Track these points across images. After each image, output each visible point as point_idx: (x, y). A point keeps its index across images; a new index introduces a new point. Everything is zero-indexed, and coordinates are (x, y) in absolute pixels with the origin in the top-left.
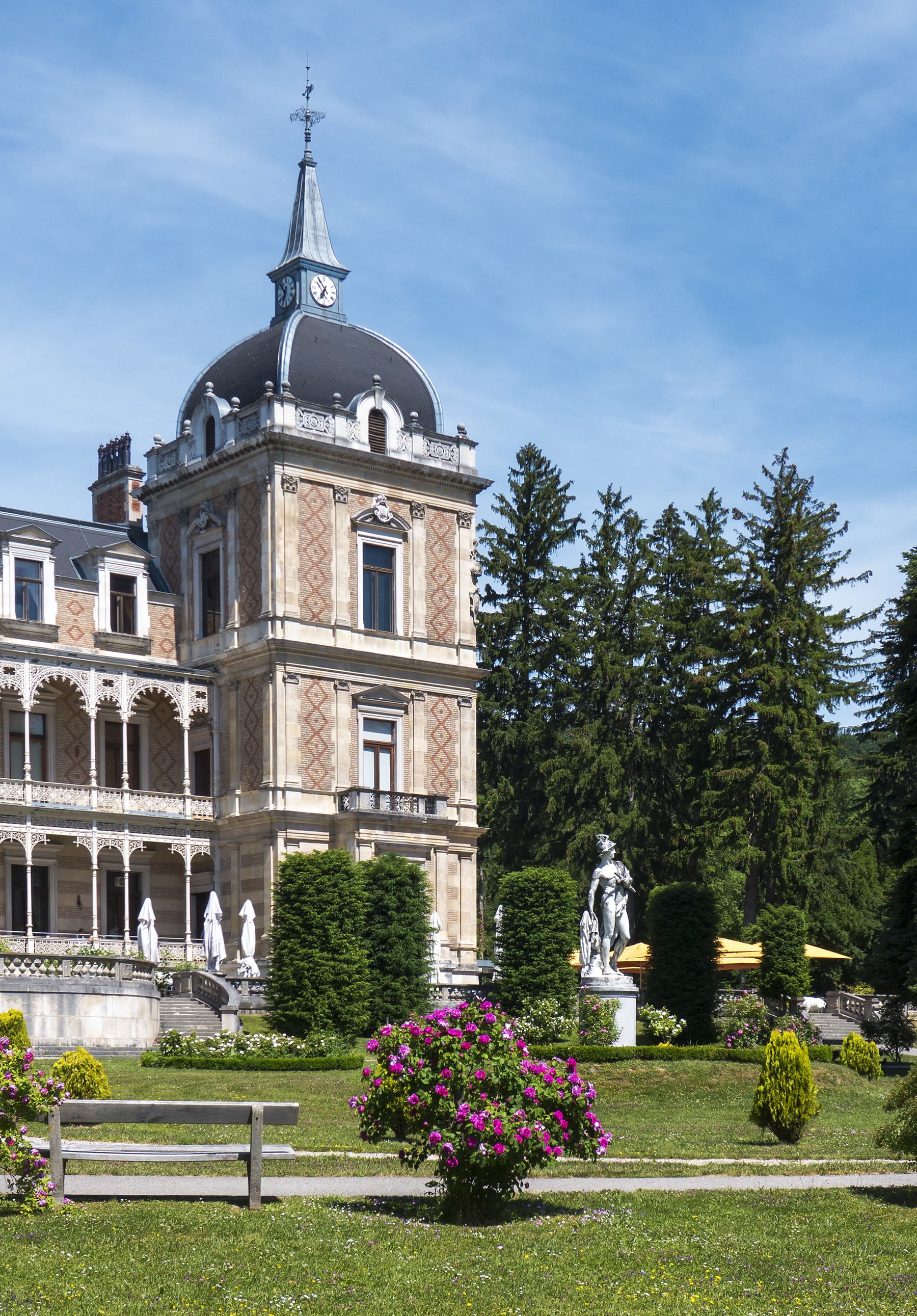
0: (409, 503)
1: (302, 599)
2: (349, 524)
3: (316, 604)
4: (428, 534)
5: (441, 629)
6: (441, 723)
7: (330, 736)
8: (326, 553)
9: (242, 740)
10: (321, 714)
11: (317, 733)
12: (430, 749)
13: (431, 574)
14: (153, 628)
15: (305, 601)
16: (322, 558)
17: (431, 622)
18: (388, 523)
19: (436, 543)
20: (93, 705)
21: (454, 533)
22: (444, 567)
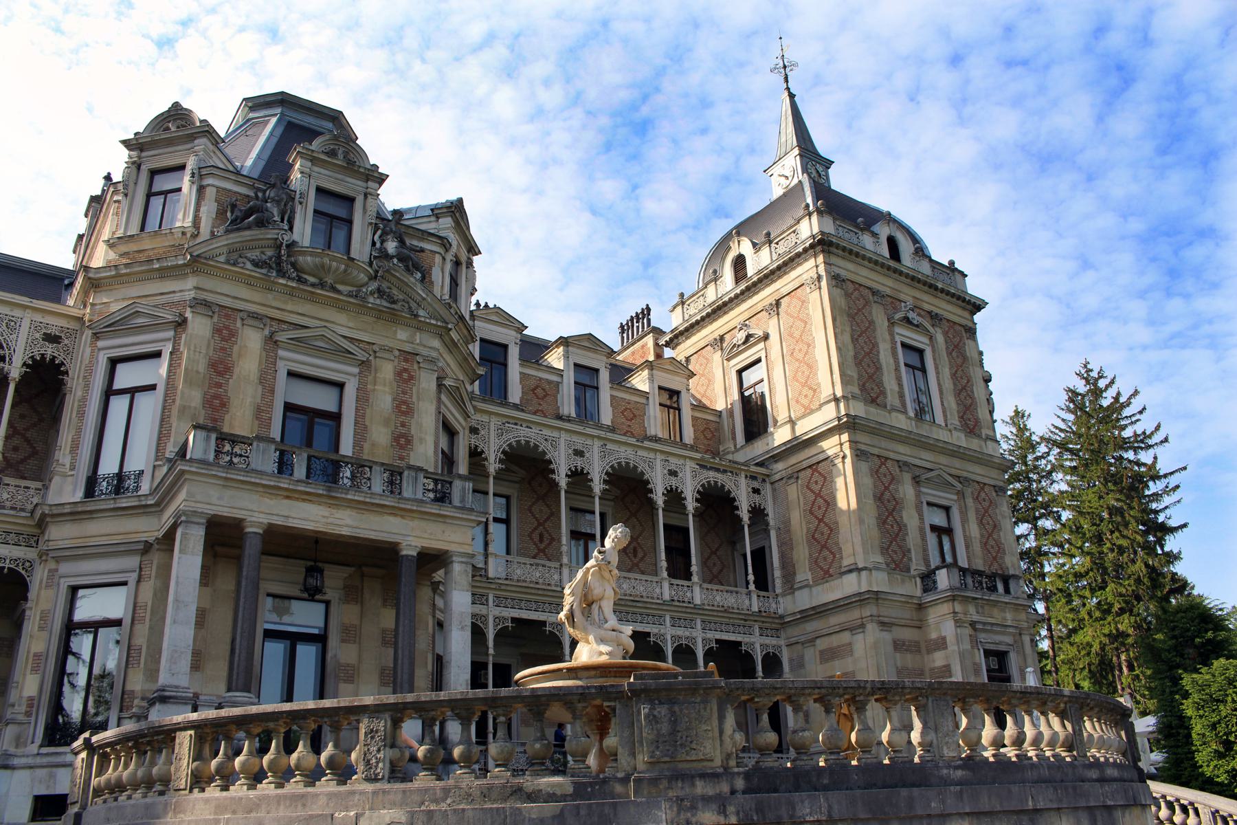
0: (930, 313)
1: (861, 383)
2: (886, 324)
3: (872, 389)
4: (946, 342)
5: (971, 423)
6: (986, 511)
7: (902, 517)
8: (874, 347)
9: (808, 529)
10: (892, 494)
11: (891, 514)
12: (982, 536)
13: (954, 376)
14: (696, 438)
15: (864, 385)
16: (871, 350)
17: (962, 417)
18: (917, 326)
19: (953, 350)
20: (660, 494)
21: (964, 344)
22: (962, 370)
